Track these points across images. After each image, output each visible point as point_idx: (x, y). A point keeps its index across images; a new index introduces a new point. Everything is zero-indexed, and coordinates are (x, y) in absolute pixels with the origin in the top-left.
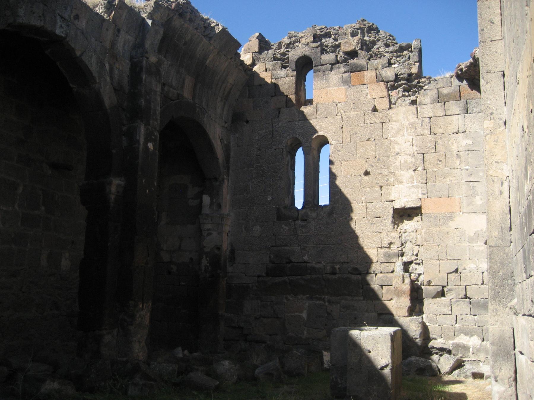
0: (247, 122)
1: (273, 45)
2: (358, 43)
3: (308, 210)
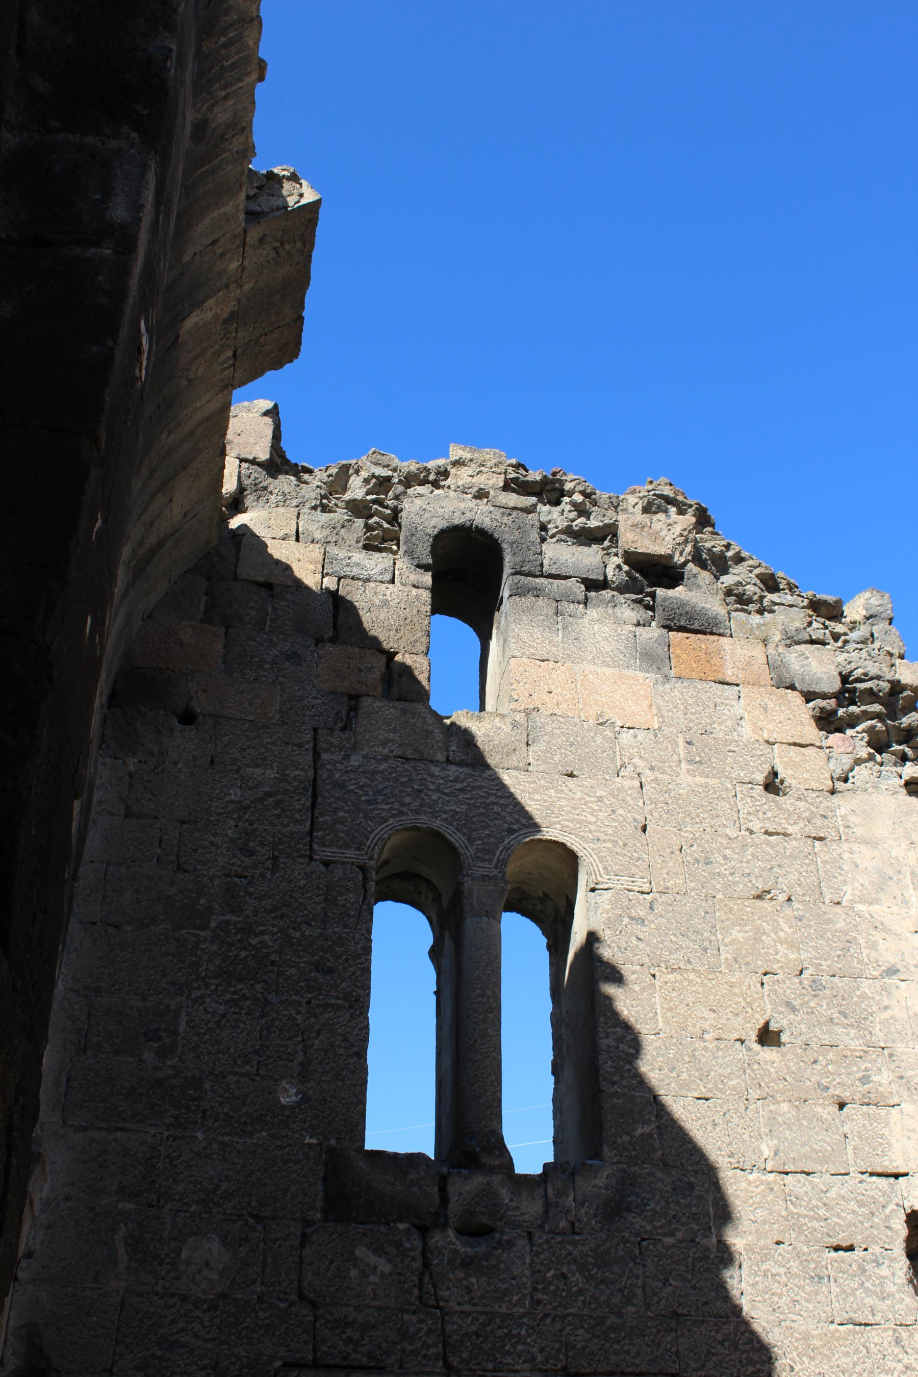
0: (188, 718)
1: (310, 472)
2: (686, 541)
3: (496, 1179)
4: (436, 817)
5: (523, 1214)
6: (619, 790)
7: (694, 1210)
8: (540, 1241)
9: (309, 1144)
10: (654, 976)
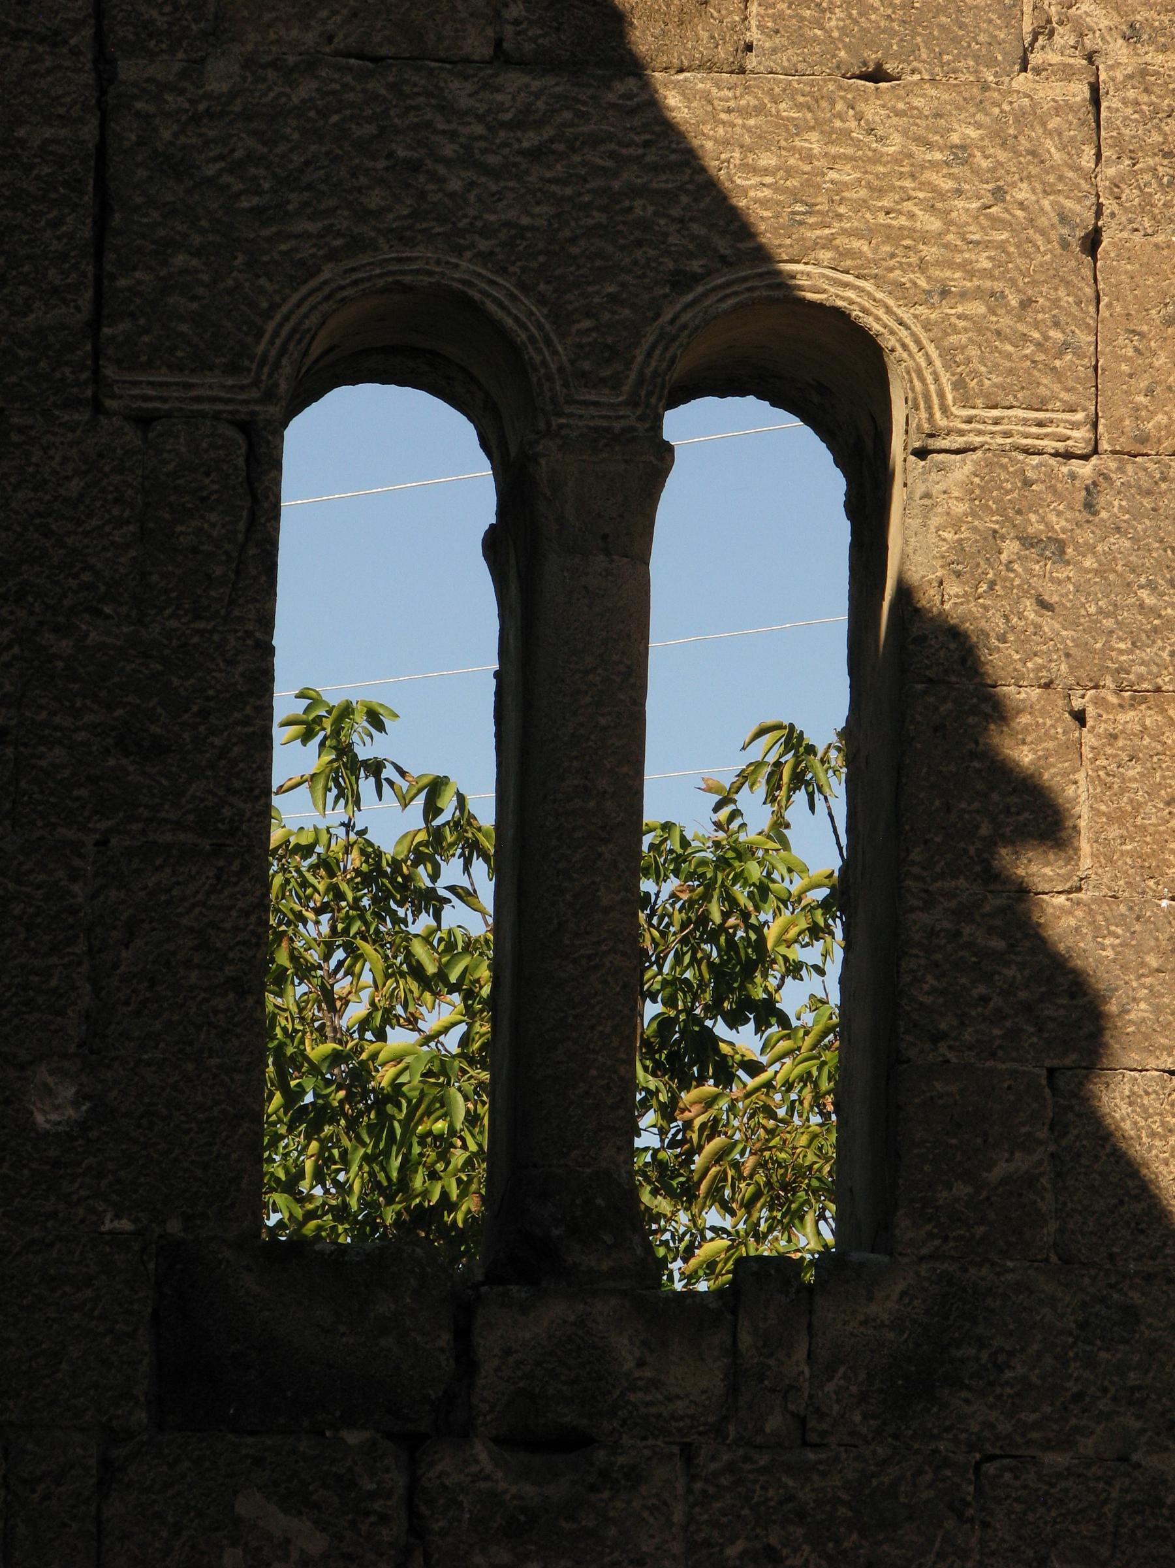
4: (459, 251)
5: (670, 1399)
6: (1021, 117)
7: (1133, 1378)
8: (713, 1466)
9: (111, 1232)
10: (1080, 717)
